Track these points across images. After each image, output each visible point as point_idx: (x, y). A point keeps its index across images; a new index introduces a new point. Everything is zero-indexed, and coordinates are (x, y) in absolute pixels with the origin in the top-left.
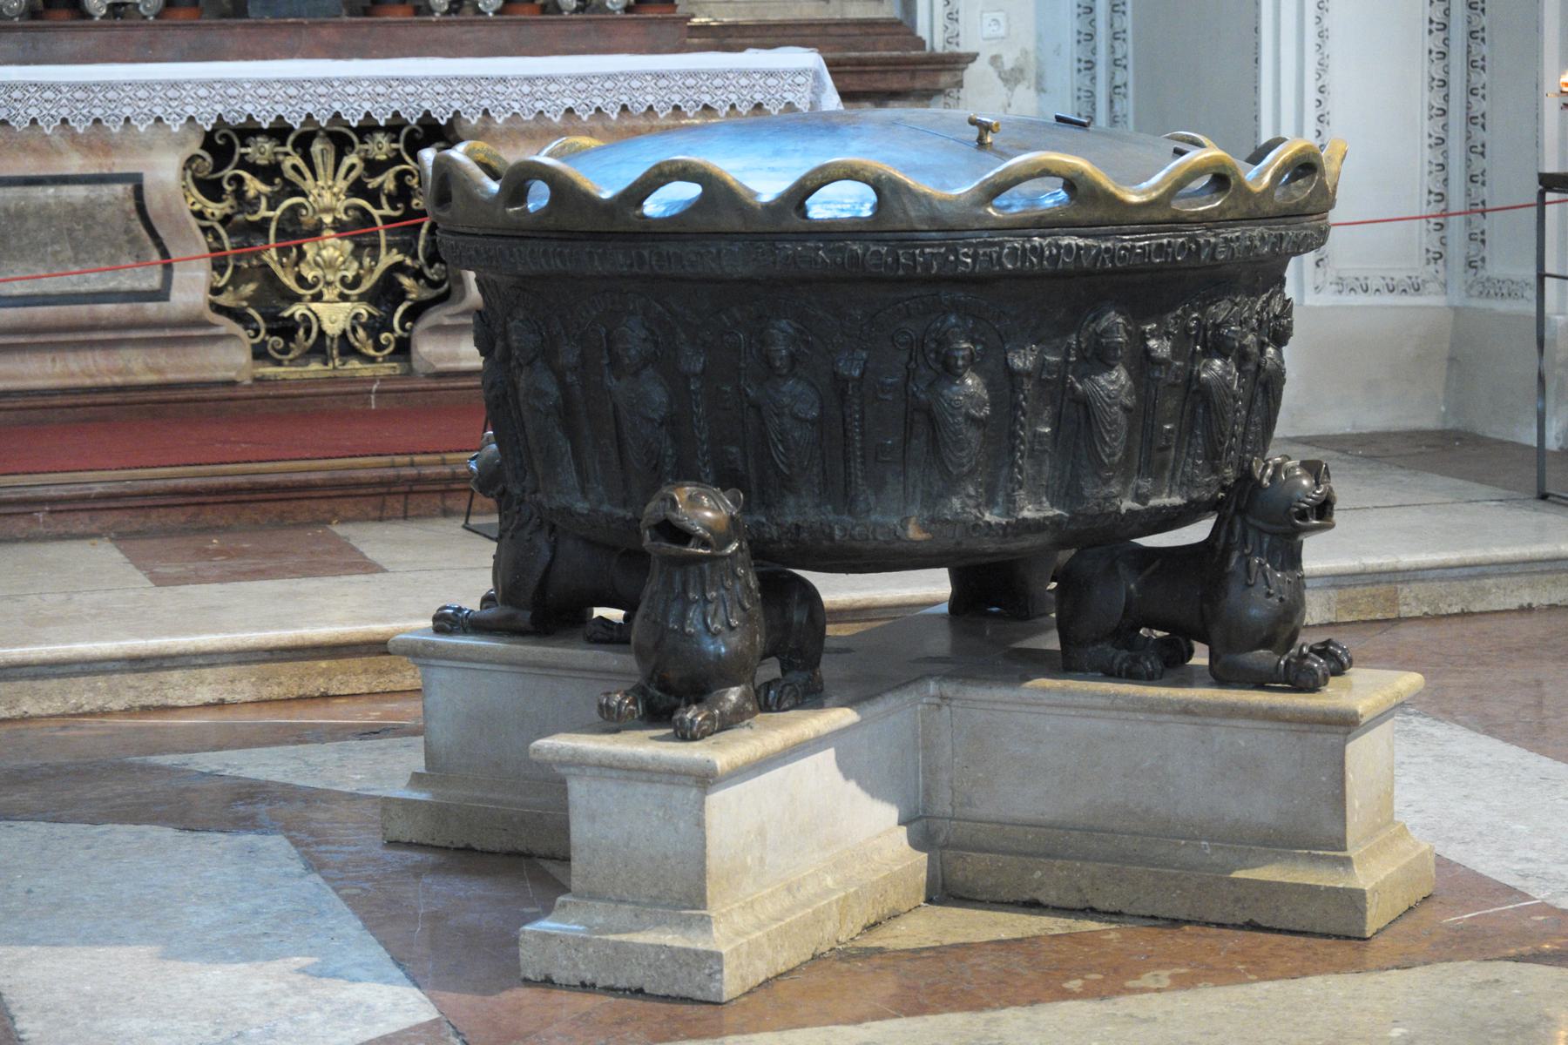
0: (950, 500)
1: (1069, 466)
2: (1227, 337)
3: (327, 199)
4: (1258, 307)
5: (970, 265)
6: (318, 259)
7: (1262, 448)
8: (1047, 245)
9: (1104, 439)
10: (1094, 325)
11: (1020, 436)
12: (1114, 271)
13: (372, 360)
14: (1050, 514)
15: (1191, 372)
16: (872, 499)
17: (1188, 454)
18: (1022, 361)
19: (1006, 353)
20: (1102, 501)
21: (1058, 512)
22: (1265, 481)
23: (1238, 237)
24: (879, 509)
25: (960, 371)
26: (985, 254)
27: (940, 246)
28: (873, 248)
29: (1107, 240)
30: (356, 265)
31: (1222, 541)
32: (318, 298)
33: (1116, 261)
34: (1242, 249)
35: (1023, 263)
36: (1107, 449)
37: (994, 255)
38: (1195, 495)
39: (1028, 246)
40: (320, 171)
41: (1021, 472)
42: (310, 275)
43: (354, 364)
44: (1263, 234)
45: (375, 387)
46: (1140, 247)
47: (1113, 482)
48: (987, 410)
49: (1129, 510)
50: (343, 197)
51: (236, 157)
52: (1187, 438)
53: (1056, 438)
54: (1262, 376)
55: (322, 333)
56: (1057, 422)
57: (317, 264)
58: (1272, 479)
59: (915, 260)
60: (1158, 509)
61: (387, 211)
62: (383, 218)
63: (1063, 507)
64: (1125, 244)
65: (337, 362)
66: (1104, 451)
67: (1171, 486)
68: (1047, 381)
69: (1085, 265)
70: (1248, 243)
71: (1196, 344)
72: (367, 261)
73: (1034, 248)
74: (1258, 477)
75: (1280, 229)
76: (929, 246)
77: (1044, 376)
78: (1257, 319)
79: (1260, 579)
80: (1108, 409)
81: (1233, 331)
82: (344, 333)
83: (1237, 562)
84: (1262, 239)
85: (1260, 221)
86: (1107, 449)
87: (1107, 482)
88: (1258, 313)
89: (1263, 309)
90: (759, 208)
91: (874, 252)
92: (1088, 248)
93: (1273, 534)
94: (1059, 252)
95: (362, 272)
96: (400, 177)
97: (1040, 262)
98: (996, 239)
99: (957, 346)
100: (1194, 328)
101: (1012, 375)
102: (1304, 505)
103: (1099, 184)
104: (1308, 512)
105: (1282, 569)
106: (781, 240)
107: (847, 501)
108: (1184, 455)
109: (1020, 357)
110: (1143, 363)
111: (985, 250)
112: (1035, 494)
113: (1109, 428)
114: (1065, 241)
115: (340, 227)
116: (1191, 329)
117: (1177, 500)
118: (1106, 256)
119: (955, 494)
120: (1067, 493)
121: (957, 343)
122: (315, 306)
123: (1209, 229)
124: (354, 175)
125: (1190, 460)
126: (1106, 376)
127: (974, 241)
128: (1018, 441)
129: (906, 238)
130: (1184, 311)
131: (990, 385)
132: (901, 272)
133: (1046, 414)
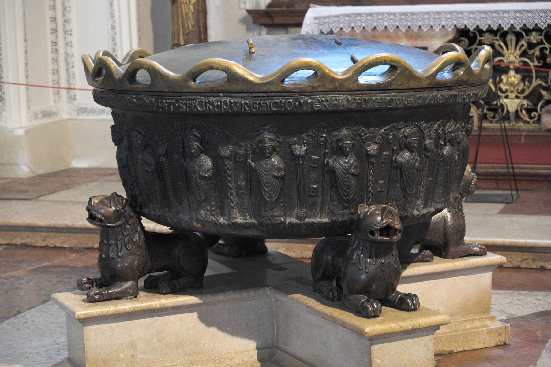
0: (200, 211)
3: (512, 58)
6: (508, 82)
8: (215, 101)
9: (265, 190)
11: (228, 185)
13: (529, 123)
16: (179, 207)
17: (331, 200)
24: (182, 212)
27: (173, 99)
28: (150, 99)
29: (247, 99)
30: (522, 85)
32: (507, 97)
33: (252, 109)
36: (267, 195)
37: (193, 104)
38: (334, 219)
39: (207, 101)
40: (510, 47)
42: (504, 88)
43: (521, 124)
44: (348, 98)
45: (524, 134)
47: (275, 210)
49: (289, 223)
50: (518, 57)
51: (477, 41)
52: (330, 192)
55: (508, 111)
57: (507, 83)
59: (164, 105)
61: (536, 63)
62: (535, 66)
65: (514, 123)
66: (266, 195)
70: (336, 103)
71: (326, 148)
72: (527, 83)
73: (209, 102)
80: (264, 176)
82: (517, 111)
86: (267, 195)
87: (272, 209)
90: (117, 79)
91: (150, 100)
92: (235, 103)
94: (221, 104)
95: (525, 88)
96: (542, 50)
97: (214, 108)
98: (193, 97)
99: (190, 144)
101: (223, 158)
103: (237, 74)
104: (375, 232)
105: (370, 257)
106: (124, 94)
109: (223, 150)
111: (189, 102)
112: (243, 212)
113: (266, 185)
115: (517, 71)
119: (202, 209)
122: (506, 100)
123: (307, 96)
124: (523, 49)
127: (185, 97)
128: (228, 188)
129: (160, 95)
132: (161, 110)
133: (241, 176)
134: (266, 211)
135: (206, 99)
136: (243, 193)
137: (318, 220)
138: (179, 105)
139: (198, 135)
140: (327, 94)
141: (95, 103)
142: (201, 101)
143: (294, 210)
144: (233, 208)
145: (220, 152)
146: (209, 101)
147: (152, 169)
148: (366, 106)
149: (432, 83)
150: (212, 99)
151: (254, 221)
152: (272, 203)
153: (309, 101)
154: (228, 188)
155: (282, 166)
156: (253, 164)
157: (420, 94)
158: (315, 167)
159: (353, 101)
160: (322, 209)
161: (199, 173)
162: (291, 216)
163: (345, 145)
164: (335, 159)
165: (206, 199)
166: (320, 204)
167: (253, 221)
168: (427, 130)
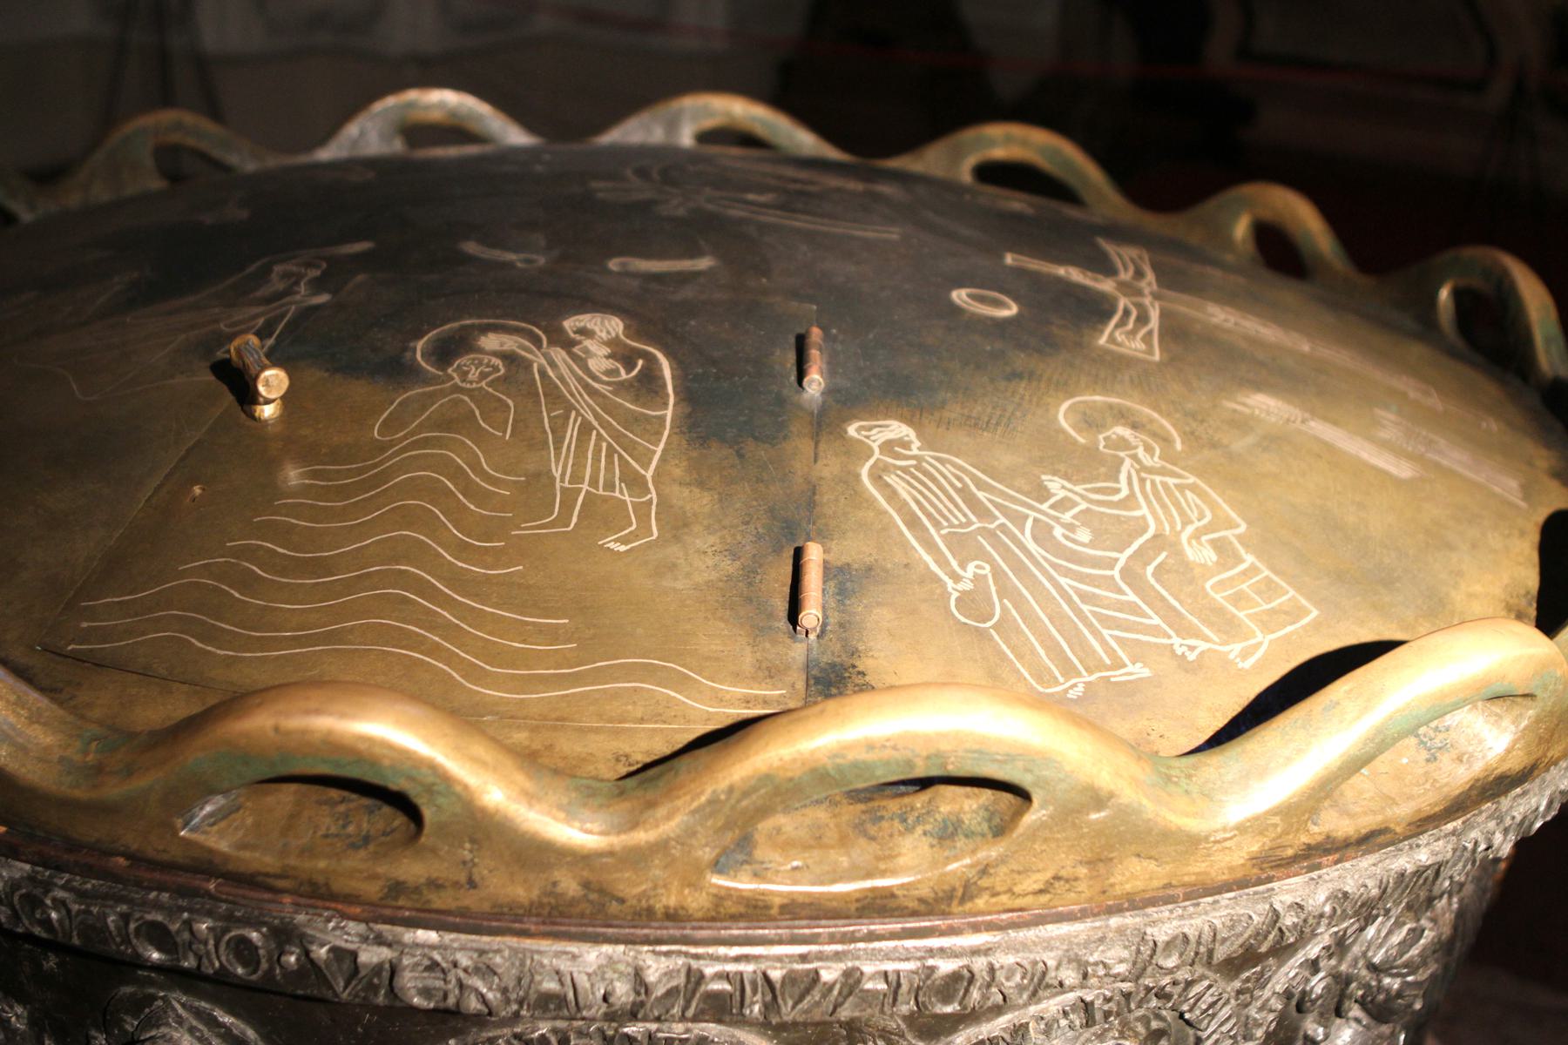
70: (550, 985)
149: (1278, 852)
157: (1181, 917)
159: (680, 980)
168: (1225, 1012)
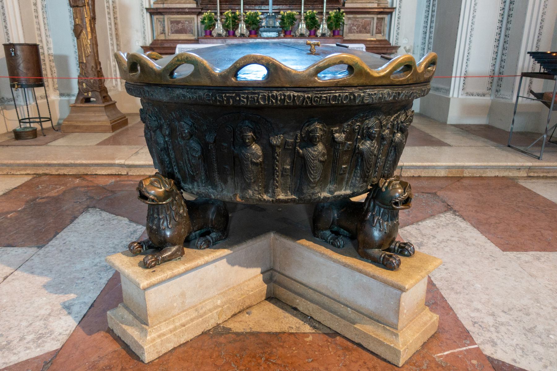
0: (248, 191)
1: (299, 181)
2: (372, 133)
4: (392, 120)
5: (246, 103)
7: (392, 169)
10: (308, 128)
11: (276, 169)
12: (312, 107)
14: (290, 197)
15: (355, 146)
16: (223, 186)
17: (354, 175)
18: (276, 141)
19: (269, 137)
20: (311, 195)
21: (294, 197)
22: (384, 189)
23: (375, 94)
25: (249, 144)
26: (251, 97)
27: (233, 93)
29: (309, 93)
31: (366, 207)
34: (377, 98)
35: (269, 102)
36: (312, 176)
37: (256, 98)
41: (277, 182)
44: (389, 92)
46: (325, 97)
48: (261, 160)
49: (325, 197)
52: (354, 170)
53: (293, 170)
54: (393, 144)
56: (293, 164)
58: (387, 188)
59: (223, 99)
60: (339, 196)
63: (296, 195)
64: (317, 95)
67: (346, 187)
68: (287, 149)
69: (298, 103)
70: (381, 96)
71: (358, 135)
73: (273, 96)
74: (381, 186)
75: (399, 90)
76: (228, 93)
77: (286, 147)
78: (391, 124)
79: (378, 225)
81: (376, 131)
83: (370, 217)
84: (389, 94)
85: (388, 87)
86: (312, 176)
87: (313, 188)
88: (392, 122)
89: (394, 120)
92: (299, 97)
93: (385, 208)
94: (284, 98)
97: (276, 102)
98: (256, 91)
100: (357, 129)
101: (273, 147)
102: (397, 200)
107: (214, 186)
108: (352, 175)
110: (331, 143)
112: (285, 190)
114: (287, 93)
116: (356, 129)
117: (348, 192)
118: (307, 100)
120: (298, 190)
121: (246, 133)
123: (360, 90)
125: (355, 178)
126: (312, 148)
127: (247, 91)
128: (276, 171)
130: (352, 123)
131: (263, 150)
132: (218, 103)
133: (288, 161)
134: (308, 189)
135: (269, 93)
136: (287, 175)
137: (343, 192)
138: (240, 99)
139: (251, 126)
140: (375, 88)
141: (128, 94)
142: (264, 95)
143: (327, 187)
144: (277, 187)
145: (272, 140)
146: (273, 95)
147: (199, 155)
148: (398, 98)
150: (275, 93)
151: (295, 197)
152: (315, 183)
153: (362, 94)
154: (276, 171)
155: (325, 151)
156: (301, 151)
158: (348, 151)
160: (347, 183)
161: (251, 160)
162: (324, 191)
163: (374, 132)
164: (362, 143)
165: (254, 182)
166: (346, 180)
167: (294, 197)
